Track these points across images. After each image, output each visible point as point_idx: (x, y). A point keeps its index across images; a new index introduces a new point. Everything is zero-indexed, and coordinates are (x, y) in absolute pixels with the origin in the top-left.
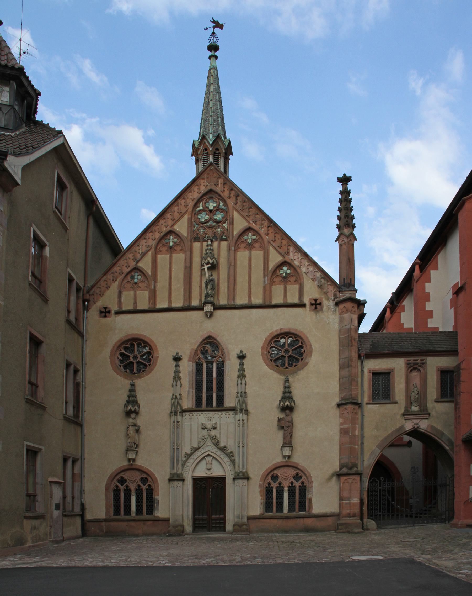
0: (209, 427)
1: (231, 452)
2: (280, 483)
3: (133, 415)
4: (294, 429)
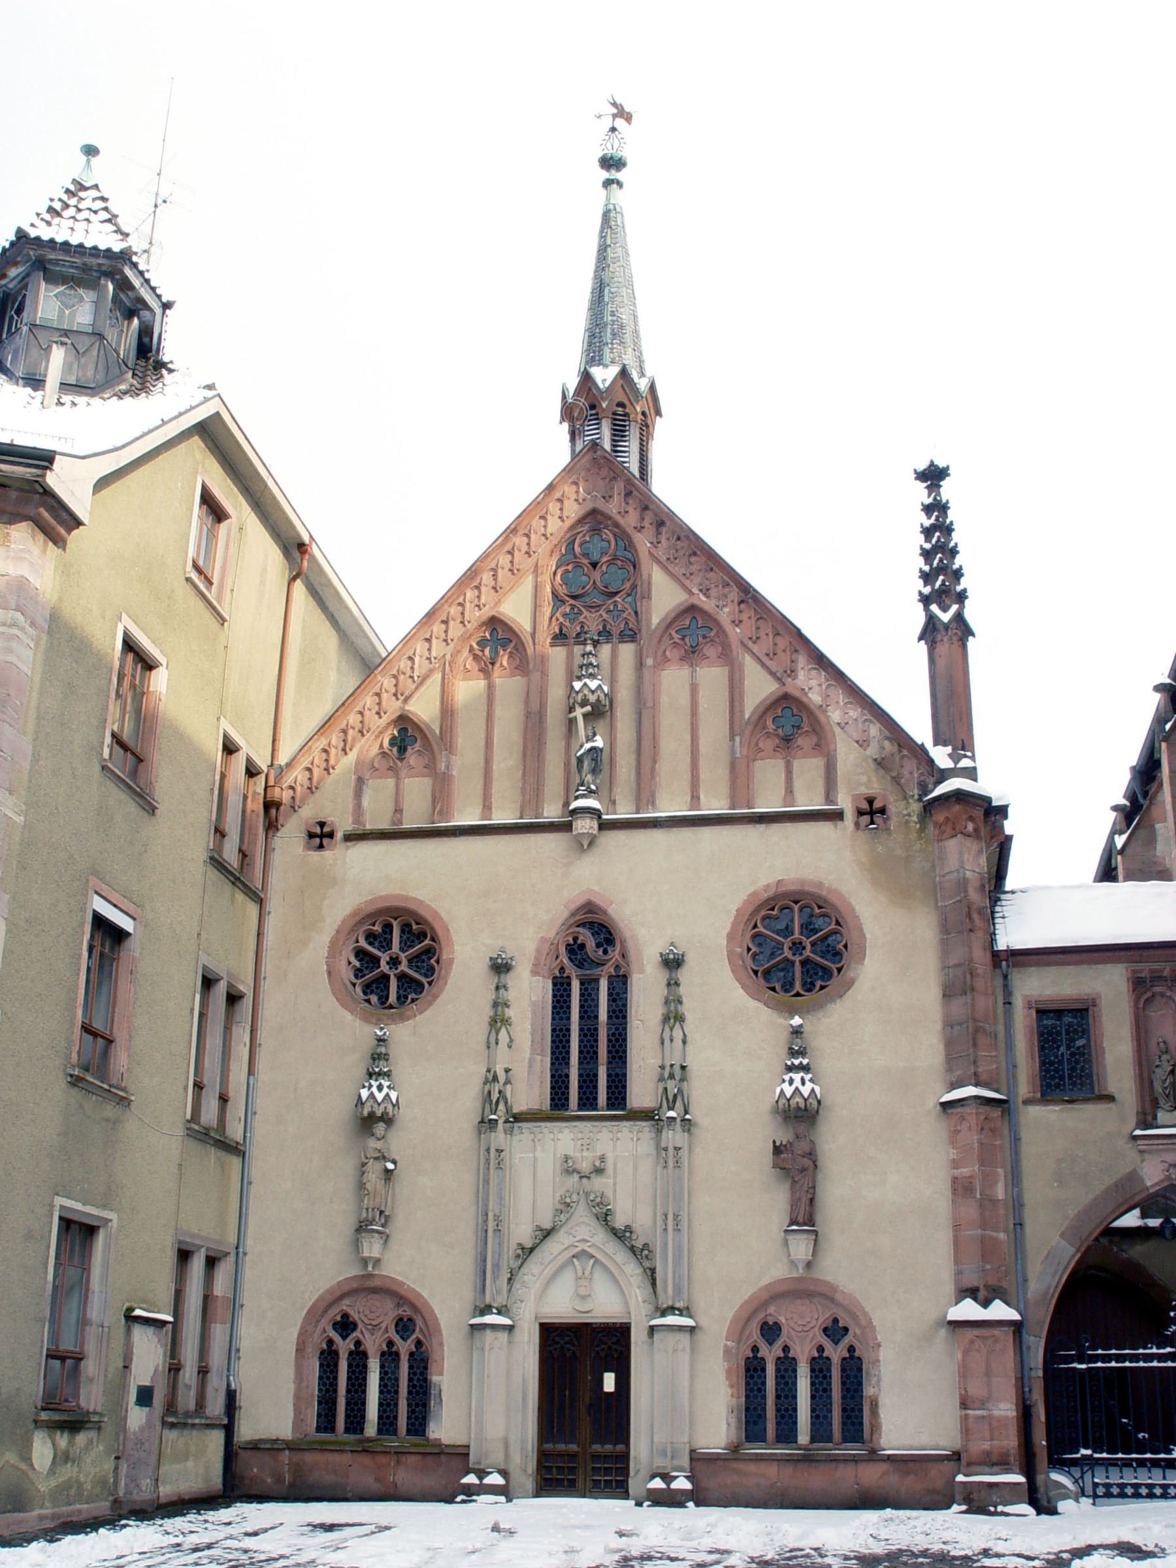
0: (585, 1167)
1: (646, 1245)
2: (786, 1349)
3: (380, 1128)
4: (820, 1176)
